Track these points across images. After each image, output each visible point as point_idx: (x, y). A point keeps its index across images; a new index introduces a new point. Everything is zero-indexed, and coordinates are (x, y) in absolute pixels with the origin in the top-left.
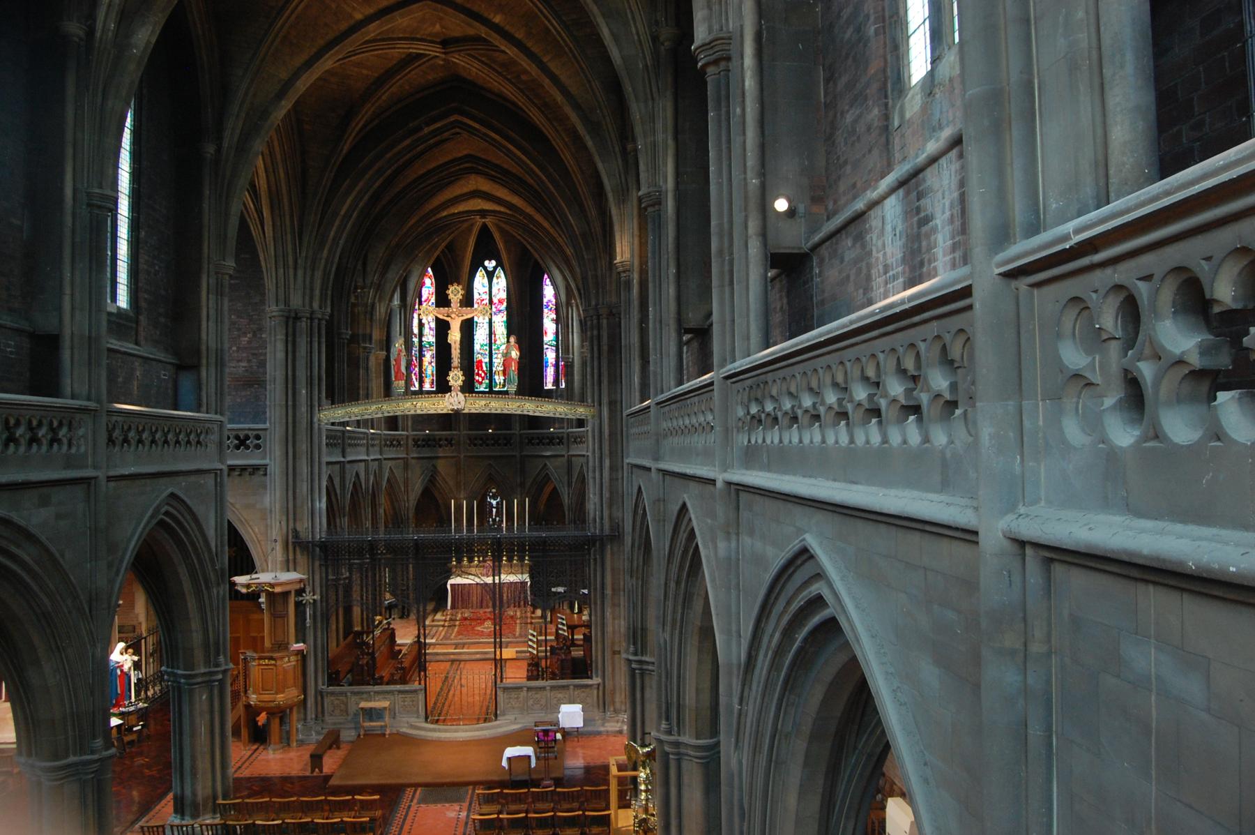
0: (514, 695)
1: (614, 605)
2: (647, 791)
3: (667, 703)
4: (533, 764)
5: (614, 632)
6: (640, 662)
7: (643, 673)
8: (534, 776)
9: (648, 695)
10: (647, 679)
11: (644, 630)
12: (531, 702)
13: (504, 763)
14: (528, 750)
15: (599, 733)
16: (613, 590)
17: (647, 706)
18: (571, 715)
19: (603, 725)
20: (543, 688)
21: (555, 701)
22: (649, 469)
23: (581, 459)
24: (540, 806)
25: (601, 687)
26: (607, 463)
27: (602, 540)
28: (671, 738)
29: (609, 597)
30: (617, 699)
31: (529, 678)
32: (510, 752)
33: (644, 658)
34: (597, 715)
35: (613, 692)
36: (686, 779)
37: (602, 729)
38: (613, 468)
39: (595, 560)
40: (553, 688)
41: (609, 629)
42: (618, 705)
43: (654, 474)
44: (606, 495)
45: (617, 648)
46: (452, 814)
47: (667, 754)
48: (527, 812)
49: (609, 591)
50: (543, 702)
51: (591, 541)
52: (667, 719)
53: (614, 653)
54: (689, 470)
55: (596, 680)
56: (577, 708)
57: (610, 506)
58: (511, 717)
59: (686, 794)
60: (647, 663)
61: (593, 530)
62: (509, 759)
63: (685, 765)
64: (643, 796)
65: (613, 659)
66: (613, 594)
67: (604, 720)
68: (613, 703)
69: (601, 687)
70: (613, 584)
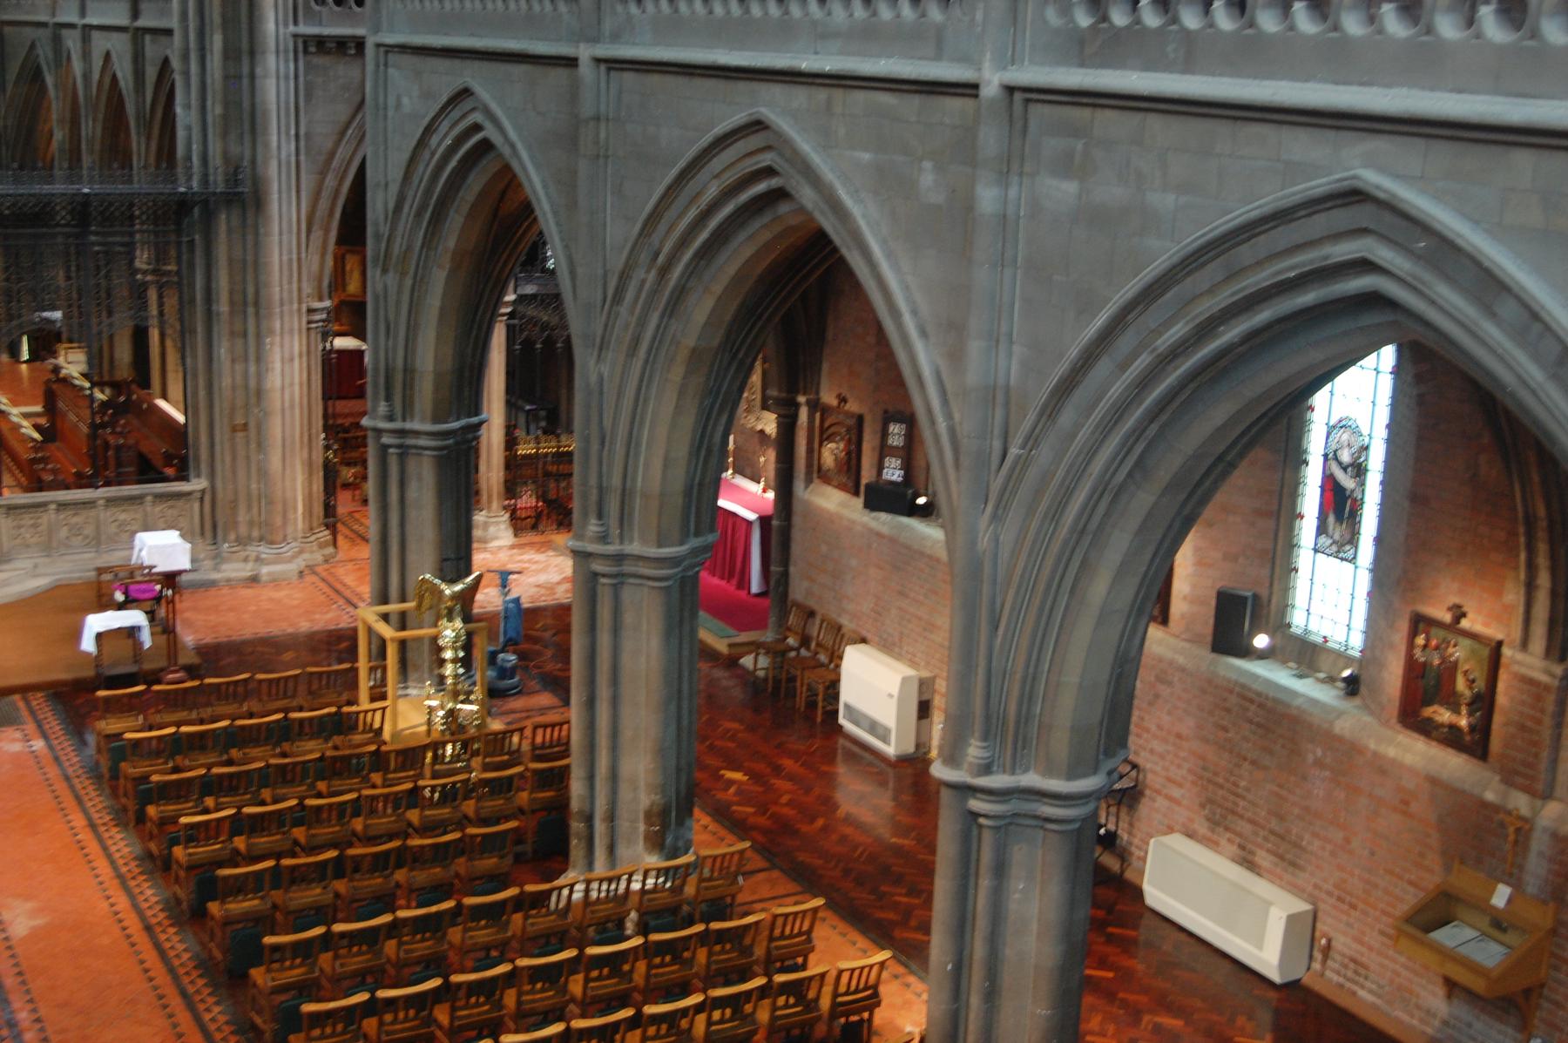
0: (27, 520)
1: (232, 334)
2: (455, 661)
3: (601, 488)
4: (146, 639)
5: (234, 388)
6: (402, 433)
7: (404, 452)
8: (147, 666)
9: (412, 493)
10: (412, 465)
11: (409, 371)
12: (64, 532)
13: (88, 644)
14: (135, 617)
15: (212, 584)
16: (232, 303)
17: (412, 514)
18: (162, 549)
19: (216, 568)
20: (89, 504)
21: (113, 528)
22: (571, 62)
23: (29, 32)
24: (254, 705)
25: (209, 498)
26: (217, 42)
27: (205, 203)
28: (611, 549)
29: (225, 317)
30: (242, 516)
31: (38, 485)
32: (98, 622)
33: (408, 425)
34: (205, 549)
35: (234, 505)
36: (628, 618)
37: (215, 576)
38: (231, 54)
39: (192, 242)
40: (111, 502)
41: (226, 382)
42: (243, 530)
43: (585, 69)
44: (215, 110)
45: (240, 420)
46: (17, 747)
47: (596, 575)
48: (286, 710)
49: (223, 307)
50: (89, 530)
51: (182, 206)
52: (600, 516)
53: (234, 429)
54: (805, 65)
55: (197, 484)
56: (171, 537)
57: (225, 135)
58: (28, 564)
59: (628, 645)
60: (417, 433)
61: (189, 184)
62: (100, 637)
63: (628, 594)
64: (449, 670)
65: (232, 439)
66: (232, 313)
67: (218, 559)
68: (236, 523)
69: (209, 498)
70: (231, 293)
